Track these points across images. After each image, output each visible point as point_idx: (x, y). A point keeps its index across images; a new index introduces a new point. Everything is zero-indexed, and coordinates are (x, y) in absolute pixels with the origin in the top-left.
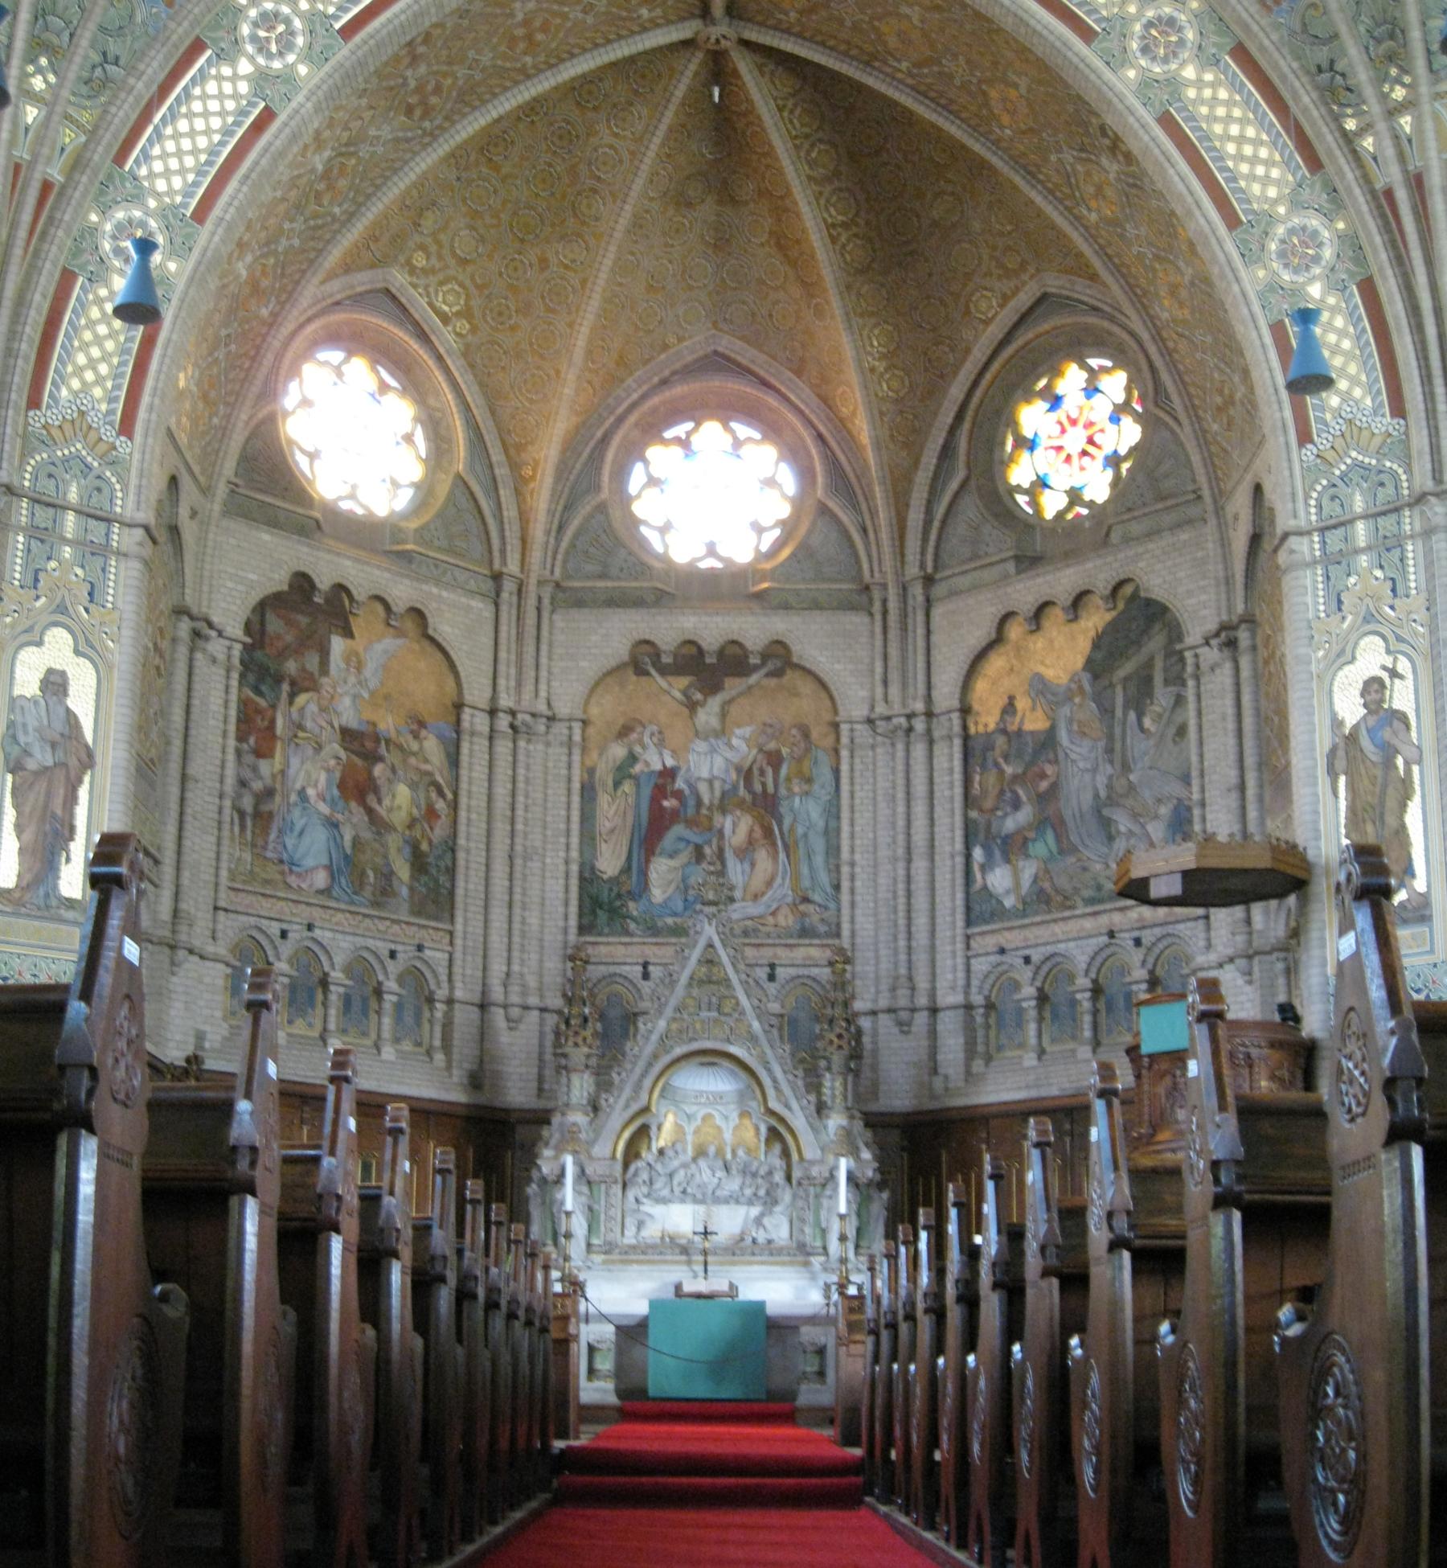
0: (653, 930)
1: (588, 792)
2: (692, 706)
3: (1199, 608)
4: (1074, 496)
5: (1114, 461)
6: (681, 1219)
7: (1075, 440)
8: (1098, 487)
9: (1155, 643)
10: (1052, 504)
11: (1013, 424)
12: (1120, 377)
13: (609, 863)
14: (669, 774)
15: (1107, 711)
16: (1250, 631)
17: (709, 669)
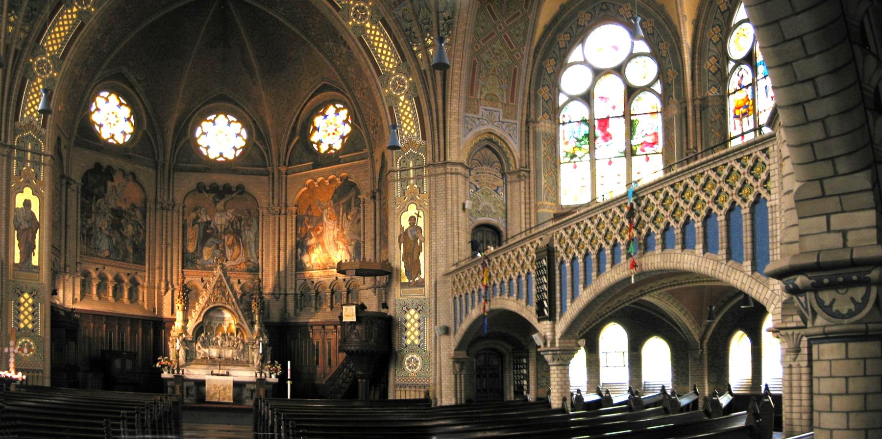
0: (204, 268)
1: (184, 227)
2: (216, 203)
3: (365, 185)
4: (330, 147)
5: (342, 137)
6: (214, 352)
7: (331, 130)
8: (338, 146)
9: (352, 193)
10: (324, 148)
11: (313, 123)
12: (345, 111)
13: (191, 248)
14: (209, 223)
15: (338, 213)
16: (380, 194)
17: (221, 192)
